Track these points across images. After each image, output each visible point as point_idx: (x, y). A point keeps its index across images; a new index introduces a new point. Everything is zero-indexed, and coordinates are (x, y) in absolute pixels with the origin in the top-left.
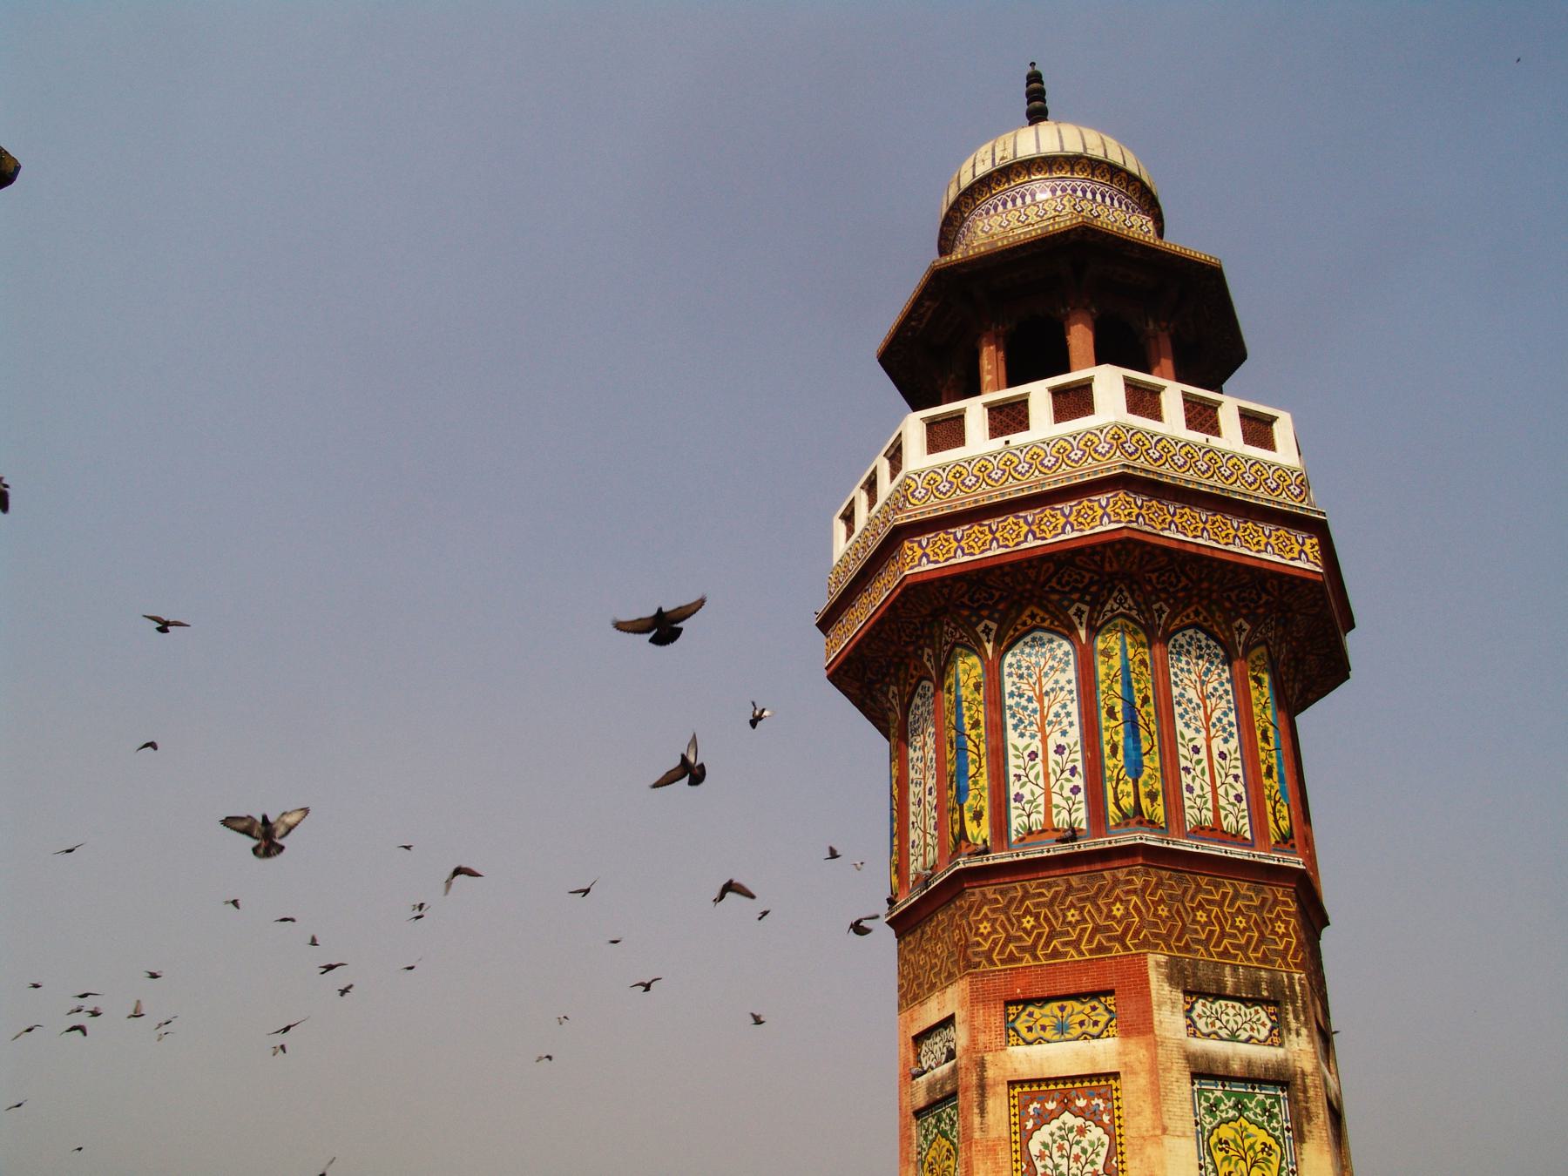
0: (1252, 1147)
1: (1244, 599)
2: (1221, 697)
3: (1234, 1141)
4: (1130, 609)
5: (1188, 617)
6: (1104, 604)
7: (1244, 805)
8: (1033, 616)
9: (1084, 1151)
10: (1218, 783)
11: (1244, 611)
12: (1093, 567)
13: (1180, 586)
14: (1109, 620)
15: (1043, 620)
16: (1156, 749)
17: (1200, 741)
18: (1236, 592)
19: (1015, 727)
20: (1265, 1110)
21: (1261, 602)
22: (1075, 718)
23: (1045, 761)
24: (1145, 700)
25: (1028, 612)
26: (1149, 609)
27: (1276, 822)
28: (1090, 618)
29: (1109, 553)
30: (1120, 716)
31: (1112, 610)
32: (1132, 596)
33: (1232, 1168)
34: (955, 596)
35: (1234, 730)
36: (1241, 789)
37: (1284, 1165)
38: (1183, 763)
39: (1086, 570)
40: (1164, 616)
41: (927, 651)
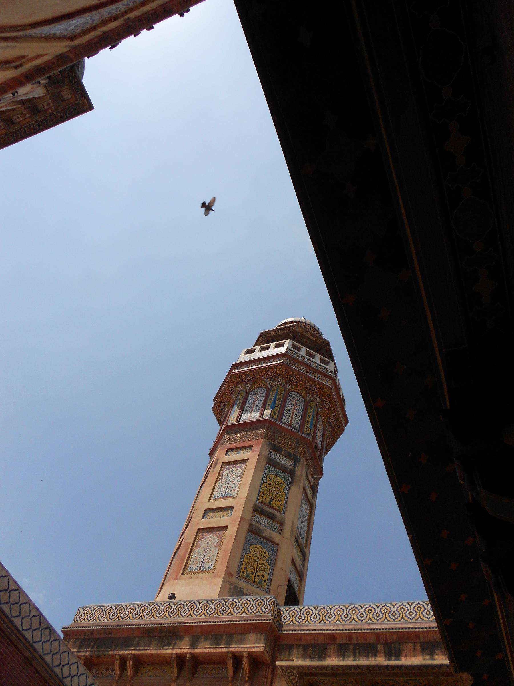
0: (278, 482)
1: (311, 389)
2: (300, 406)
3: (274, 479)
4: (282, 383)
5: (296, 390)
6: (275, 382)
7: (299, 424)
8: (259, 385)
9: (235, 474)
10: (293, 418)
11: (310, 392)
12: (274, 372)
13: (295, 381)
14: (276, 385)
15: (261, 385)
16: (279, 407)
17: (292, 410)
18: (309, 387)
19: (248, 403)
20: (284, 477)
21: (315, 391)
22: (262, 401)
23: (253, 408)
24: (280, 399)
25: (259, 384)
26: (286, 383)
27: (306, 430)
28: (272, 384)
29: (278, 368)
30: (272, 400)
31: (277, 383)
32: (283, 381)
33: (271, 483)
34: (242, 378)
35: (301, 412)
36: (299, 421)
37: (286, 488)
38: (285, 412)
39: (272, 373)
40: (290, 387)
41: (235, 394)
